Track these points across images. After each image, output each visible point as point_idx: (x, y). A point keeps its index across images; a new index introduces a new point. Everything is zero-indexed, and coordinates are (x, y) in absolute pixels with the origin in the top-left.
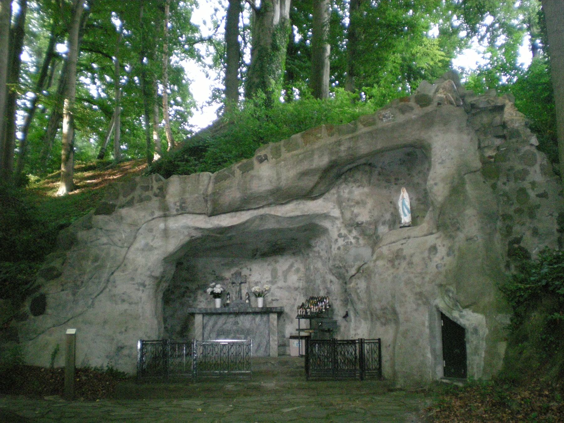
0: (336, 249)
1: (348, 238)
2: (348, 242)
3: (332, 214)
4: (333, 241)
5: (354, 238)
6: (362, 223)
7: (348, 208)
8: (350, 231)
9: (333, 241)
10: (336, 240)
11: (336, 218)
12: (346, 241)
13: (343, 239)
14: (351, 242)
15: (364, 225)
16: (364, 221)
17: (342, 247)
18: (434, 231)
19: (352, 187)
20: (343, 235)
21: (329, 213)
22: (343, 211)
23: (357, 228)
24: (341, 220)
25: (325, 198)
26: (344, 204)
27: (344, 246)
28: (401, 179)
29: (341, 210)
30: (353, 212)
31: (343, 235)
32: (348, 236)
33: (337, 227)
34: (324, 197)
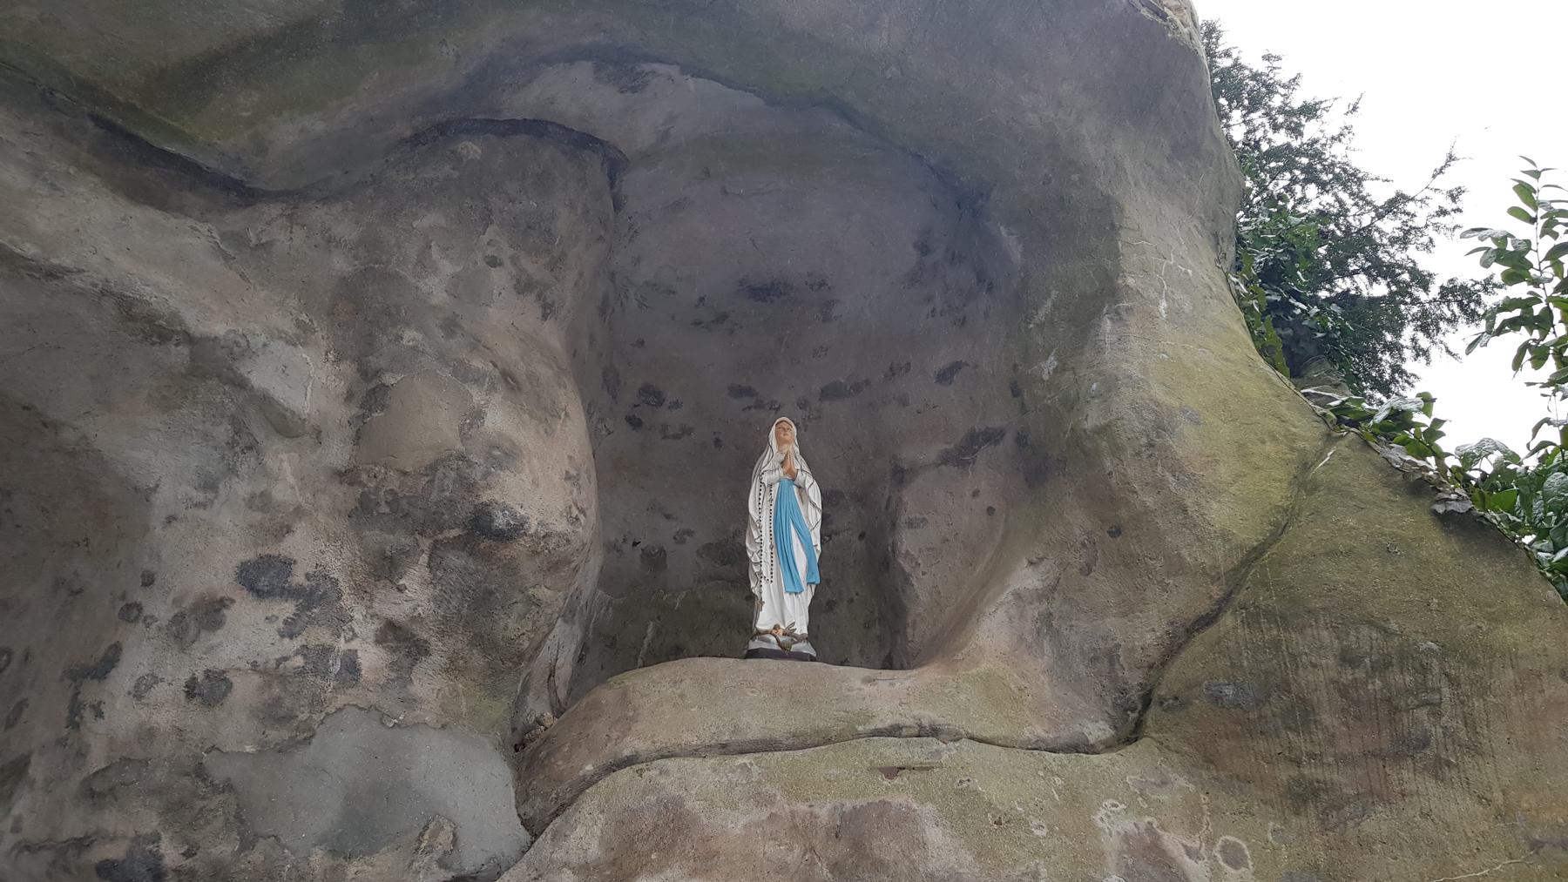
0: (168, 691)
1: (341, 621)
2: (326, 651)
3: (261, 376)
4: (160, 609)
5: (393, 633)
6: (515, 530)
7: (446, 373)
8: (386, 568)
9: (160, 609)
10: (211, 612)
11: (285, 426)
12: (320, 636)
13: (287, 609)
14: (351, 666)
15: (519, 548)
16: (533, 527)
17: (245, 689)
18: (1098, 730)
19: (494, 262)
20: (298, 578)
21: (248, 352)
22: (389, 379)
23: (455, 560)
24: (337, 453)
25: (237, 239)
26: (410, 336)
27: (272, 674)
28: (676, 405)
29: (366, 374)
30: (478, 415)
31: (298, 578)
32: (347, 601)
33: (261, 501)
34: (235, 220)
